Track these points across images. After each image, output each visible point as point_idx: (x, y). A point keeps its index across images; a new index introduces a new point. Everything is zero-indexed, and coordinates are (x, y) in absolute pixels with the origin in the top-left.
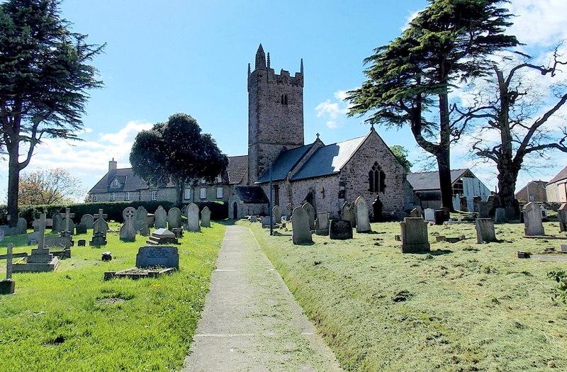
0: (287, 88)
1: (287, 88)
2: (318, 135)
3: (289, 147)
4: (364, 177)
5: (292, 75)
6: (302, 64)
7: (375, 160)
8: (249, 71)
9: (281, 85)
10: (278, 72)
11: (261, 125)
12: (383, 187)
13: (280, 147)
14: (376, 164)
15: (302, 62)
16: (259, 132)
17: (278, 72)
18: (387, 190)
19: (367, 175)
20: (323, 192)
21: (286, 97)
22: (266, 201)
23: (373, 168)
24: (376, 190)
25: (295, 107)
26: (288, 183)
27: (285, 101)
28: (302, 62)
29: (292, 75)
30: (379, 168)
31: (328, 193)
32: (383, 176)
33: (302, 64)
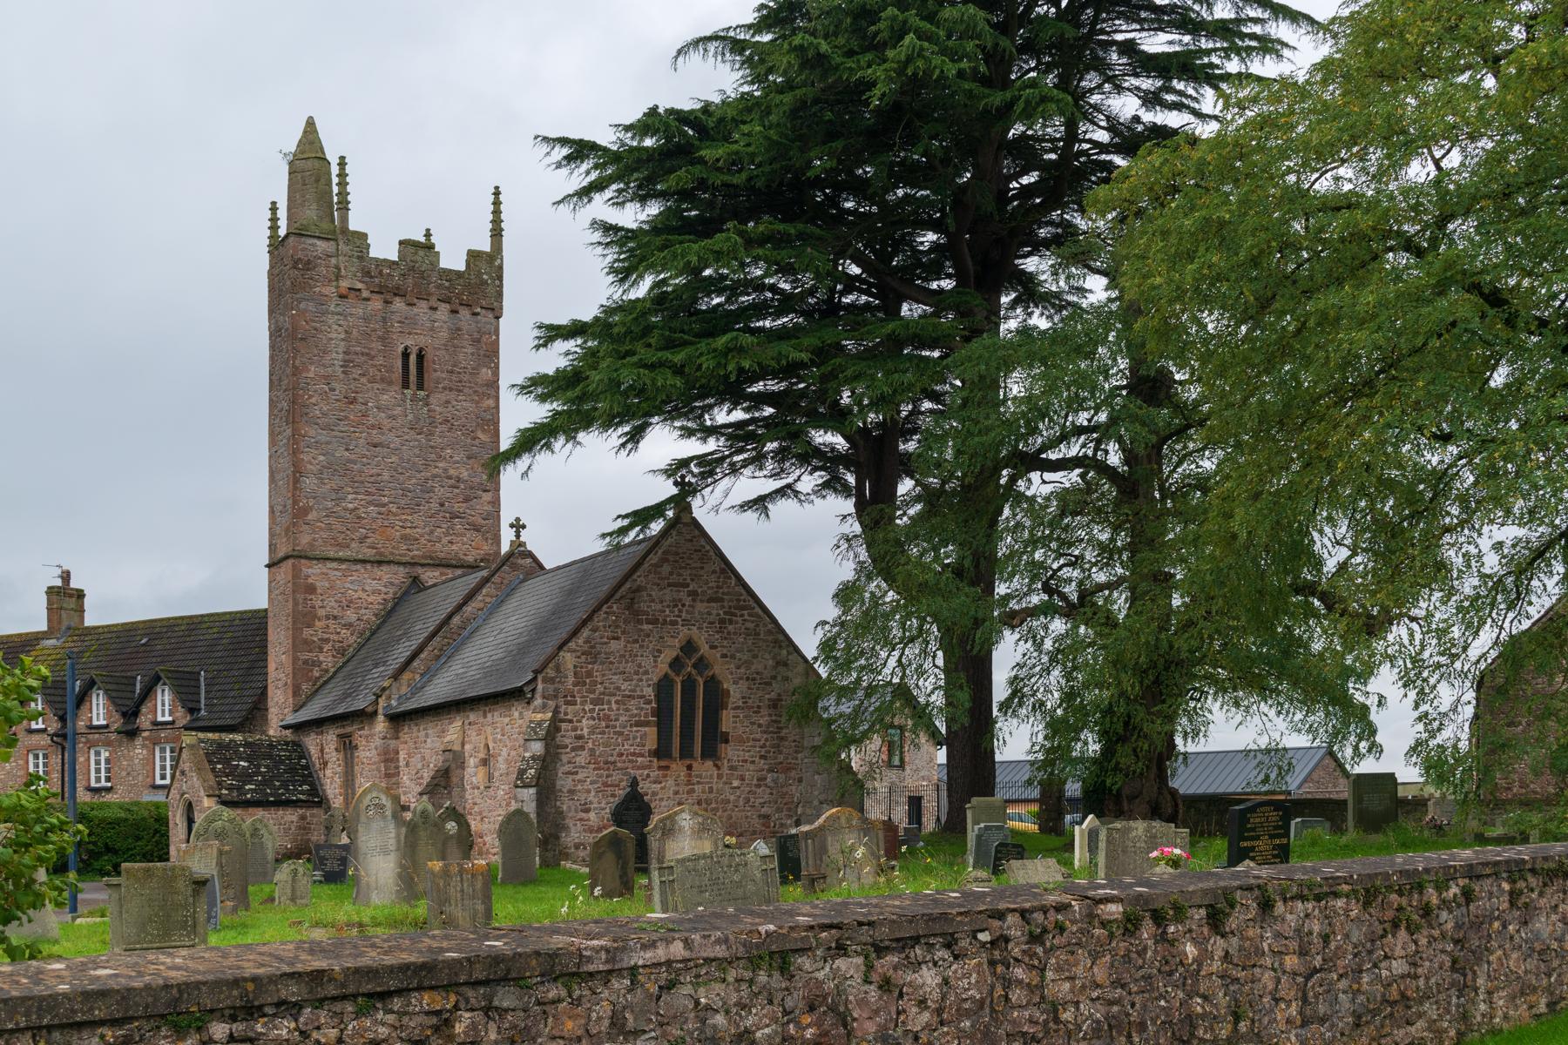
0: (429, 326)
1: (429, 326)
2: (518, 526)
3: (430, 576)
4: (632, 704)
5: (452, 259)
6: (497, 212)
7: (684, 632)
8: (274, 227)
9: (398, 304)
10: (384, 248)
11: (309, 483)
12: (714, 742)
13: (399, 575)
14: (689, 647)
15: (497, 203)
16: (300, 513)
17: (384, 248)
18: (730, 752)
19: (649, 692)
20: (485, 762)
21: (421, 357)
22: (317, 799)
23: (676, 664)
24: (686, 753)
25: (463, 405)
26: (381, 725)
27: (415, 371)
28: (497, 203)
29: (452, 259)
30: (701, 664)
31: (501, 765)
32: (716, 699)
33: (497, 212)
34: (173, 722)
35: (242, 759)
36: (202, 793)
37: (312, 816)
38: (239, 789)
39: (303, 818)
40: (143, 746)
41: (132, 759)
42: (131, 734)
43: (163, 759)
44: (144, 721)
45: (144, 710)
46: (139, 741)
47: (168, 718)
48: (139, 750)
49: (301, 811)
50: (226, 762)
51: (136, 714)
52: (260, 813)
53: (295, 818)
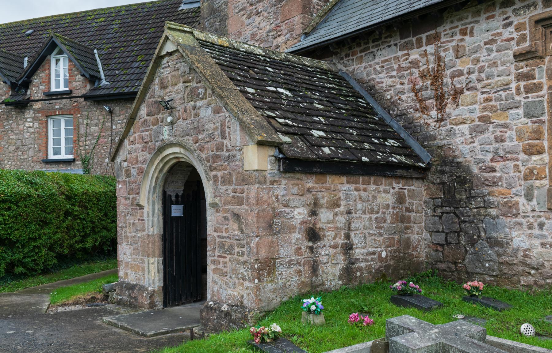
34: (70, 92)
35: (278, 84)
36: (236, 135)
37: (412, 195)
38: (305, 136)
39: (400, 199)
40: (35, 119)
41: (21, 132)
42: (21, 105)
43: (57, 133)
44: (36, 91)
45: (36, 80)
46: (29, 114)
47: (62, 88)
48: (29, 122)
49: (398, 186)
50: (259, 84)
51: (26, 85)
52: (342, 186)
53: (389, 199)
